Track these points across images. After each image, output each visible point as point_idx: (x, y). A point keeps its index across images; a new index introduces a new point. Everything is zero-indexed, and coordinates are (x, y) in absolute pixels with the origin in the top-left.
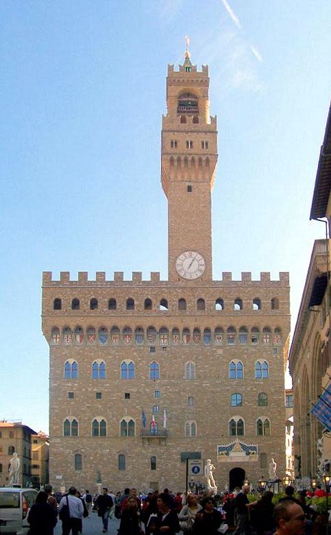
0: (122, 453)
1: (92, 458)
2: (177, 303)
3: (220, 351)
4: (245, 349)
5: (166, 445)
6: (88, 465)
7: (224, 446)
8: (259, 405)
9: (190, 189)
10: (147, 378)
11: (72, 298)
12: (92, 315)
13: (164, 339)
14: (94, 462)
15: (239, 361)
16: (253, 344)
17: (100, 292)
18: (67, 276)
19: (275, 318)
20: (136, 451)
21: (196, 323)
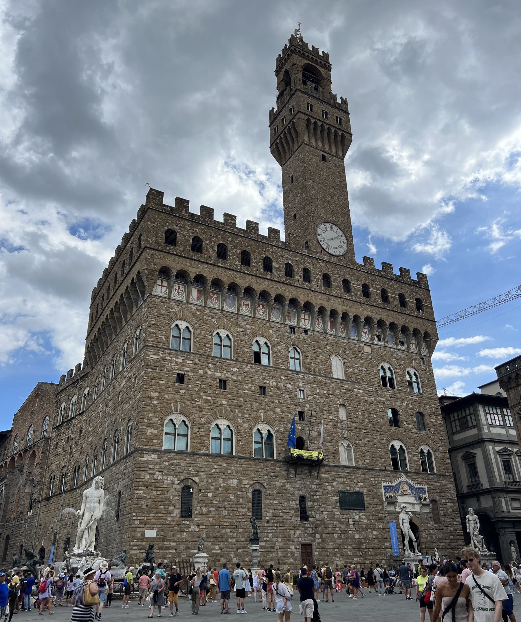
0: (257, 487)
1: (210, 495)
2: (322, 276)
3: (367, 349)
4: (394, 353)
5: (318, 477)
6: (204, 509)
7: (390, 484)
8: (419, 429)
9: (324, 158)
10: (288, 369)
11: (192, 235)
12: (219, 264)
13: (305, 319)
14: (214, 502)
16: (400, 347)
17: (230, 239)
18: (186, 204)
19: (421, 321)
20: (278, 484)
21: (344, 308)
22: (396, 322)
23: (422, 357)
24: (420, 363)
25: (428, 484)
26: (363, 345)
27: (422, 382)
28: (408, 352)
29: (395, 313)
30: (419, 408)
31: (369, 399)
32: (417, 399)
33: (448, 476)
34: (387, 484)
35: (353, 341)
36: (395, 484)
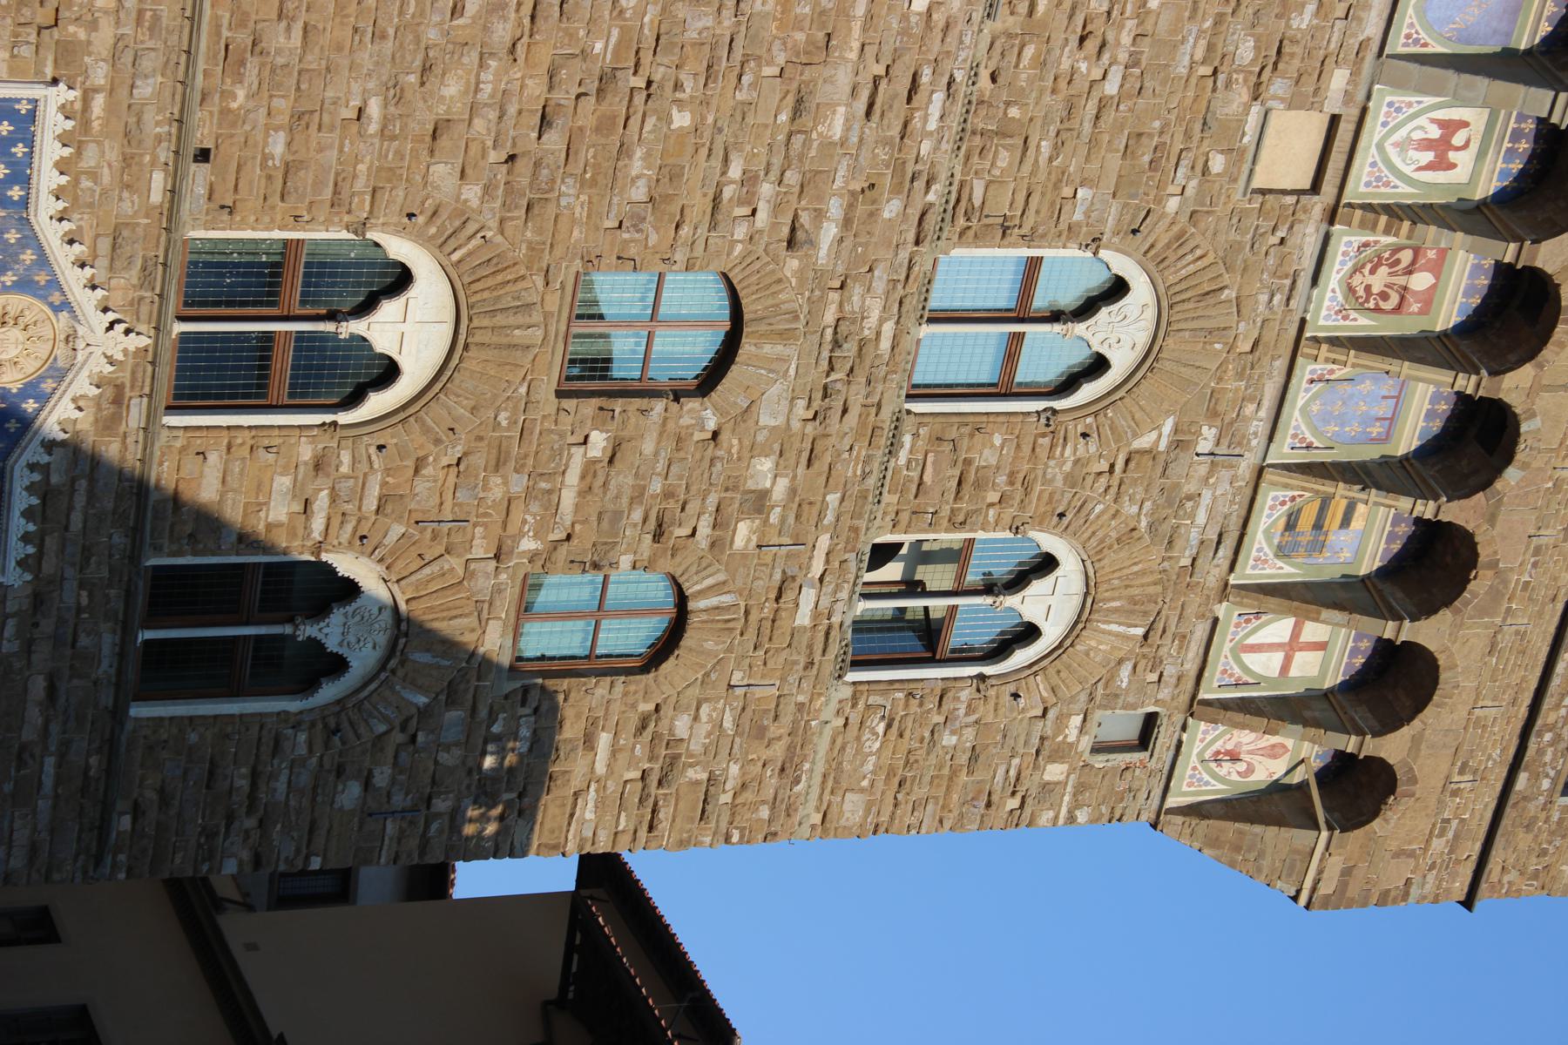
3: (1289, 151)
4: (1230, 432)
7: (47, 178)
15: (1121, 361)
22: (1512, 474)
23: (1164, 737)
24: (1112, 699)
25: (38, 600)
26: (1333, 105)
27: (944, 692)
28: (1224, 590)
30: (721, 621)
31: (844, 78)
32: (803, 618)
33: (103, 827)
34: (49, 151)
36: (51, 234)
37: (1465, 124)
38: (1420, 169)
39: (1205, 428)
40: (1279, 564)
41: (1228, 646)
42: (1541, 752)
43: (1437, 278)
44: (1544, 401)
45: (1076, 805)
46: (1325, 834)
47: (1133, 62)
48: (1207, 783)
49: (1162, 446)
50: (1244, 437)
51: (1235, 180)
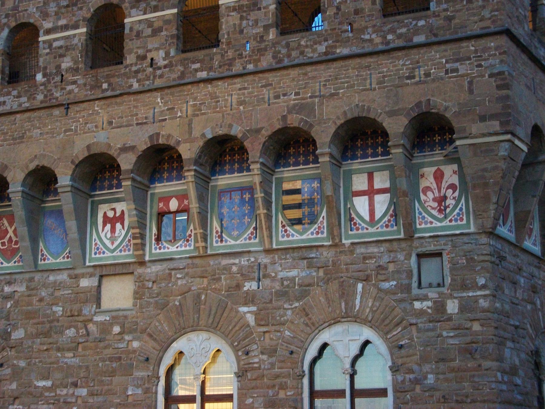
19: (401, 64)
22: (236, 131)
23: (432, 248)
28: (335, 245)
29: (238, 83)
35: (52, 278)
37: (105, 213)
38: (123, 228)
39: (245, 289)
40: (321, 219)
41: (371, 230)
42: (400, 36)
43: (171, 197)
44: (196, 133)
45: (475, 287)
46: (458, 143)
47: (75, 385)
48: (461, 209)
49: (254, 309)
50: (249, 266)
51: (126, 317)
